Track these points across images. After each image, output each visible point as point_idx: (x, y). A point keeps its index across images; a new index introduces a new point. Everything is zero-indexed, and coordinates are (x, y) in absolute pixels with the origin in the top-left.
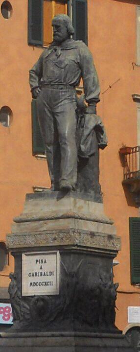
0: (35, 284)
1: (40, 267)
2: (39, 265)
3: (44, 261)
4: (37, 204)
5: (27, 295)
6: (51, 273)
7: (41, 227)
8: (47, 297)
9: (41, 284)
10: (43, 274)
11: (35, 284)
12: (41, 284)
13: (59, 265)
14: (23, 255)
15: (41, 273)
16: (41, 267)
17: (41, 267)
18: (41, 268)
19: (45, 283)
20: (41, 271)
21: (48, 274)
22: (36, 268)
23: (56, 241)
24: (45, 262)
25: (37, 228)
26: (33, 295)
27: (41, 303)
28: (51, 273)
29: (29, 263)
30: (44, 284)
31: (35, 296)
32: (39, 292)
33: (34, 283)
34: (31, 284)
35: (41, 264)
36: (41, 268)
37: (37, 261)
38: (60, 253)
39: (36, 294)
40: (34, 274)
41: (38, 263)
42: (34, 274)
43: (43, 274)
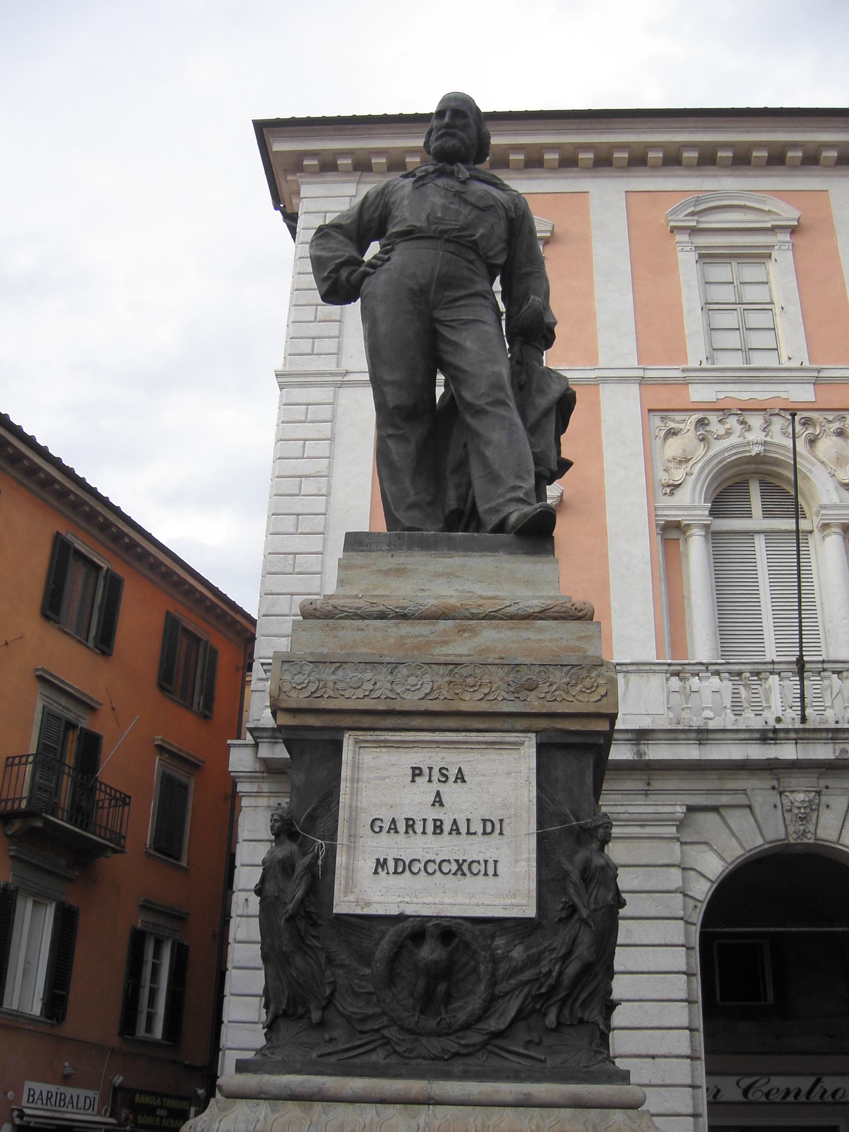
0: (403, 867)
2: (424, 791)
3: (453, 773)
4: (400, 572)
5: (358, 911)
6: (491, 827)
7: (446, 643)
8: (468, 925)
11: (403, 867)
14: (348, 742)
15: (438, 828)
16: (438, 794)
17: (438, 794)
18: (438, 801)
21: (477, 827)
22: (415, 800)
23: (532, 697)
24: (460, 777)
25: (429, 644)
26: (395, 912)
27: (429, 952)
28: (491, 827)
29: (377, 780)
30: (454, 867)
32: (429, 900)
33: (396, 860)
34: (381, 864)
35: (436, 786)
36: (438, 801)
37: (416, 772)
38: (541, 748)
39: (409, 911)
40: (401, 827)
41: (422, 781)
42: (401, 827)
43: (447, 827)
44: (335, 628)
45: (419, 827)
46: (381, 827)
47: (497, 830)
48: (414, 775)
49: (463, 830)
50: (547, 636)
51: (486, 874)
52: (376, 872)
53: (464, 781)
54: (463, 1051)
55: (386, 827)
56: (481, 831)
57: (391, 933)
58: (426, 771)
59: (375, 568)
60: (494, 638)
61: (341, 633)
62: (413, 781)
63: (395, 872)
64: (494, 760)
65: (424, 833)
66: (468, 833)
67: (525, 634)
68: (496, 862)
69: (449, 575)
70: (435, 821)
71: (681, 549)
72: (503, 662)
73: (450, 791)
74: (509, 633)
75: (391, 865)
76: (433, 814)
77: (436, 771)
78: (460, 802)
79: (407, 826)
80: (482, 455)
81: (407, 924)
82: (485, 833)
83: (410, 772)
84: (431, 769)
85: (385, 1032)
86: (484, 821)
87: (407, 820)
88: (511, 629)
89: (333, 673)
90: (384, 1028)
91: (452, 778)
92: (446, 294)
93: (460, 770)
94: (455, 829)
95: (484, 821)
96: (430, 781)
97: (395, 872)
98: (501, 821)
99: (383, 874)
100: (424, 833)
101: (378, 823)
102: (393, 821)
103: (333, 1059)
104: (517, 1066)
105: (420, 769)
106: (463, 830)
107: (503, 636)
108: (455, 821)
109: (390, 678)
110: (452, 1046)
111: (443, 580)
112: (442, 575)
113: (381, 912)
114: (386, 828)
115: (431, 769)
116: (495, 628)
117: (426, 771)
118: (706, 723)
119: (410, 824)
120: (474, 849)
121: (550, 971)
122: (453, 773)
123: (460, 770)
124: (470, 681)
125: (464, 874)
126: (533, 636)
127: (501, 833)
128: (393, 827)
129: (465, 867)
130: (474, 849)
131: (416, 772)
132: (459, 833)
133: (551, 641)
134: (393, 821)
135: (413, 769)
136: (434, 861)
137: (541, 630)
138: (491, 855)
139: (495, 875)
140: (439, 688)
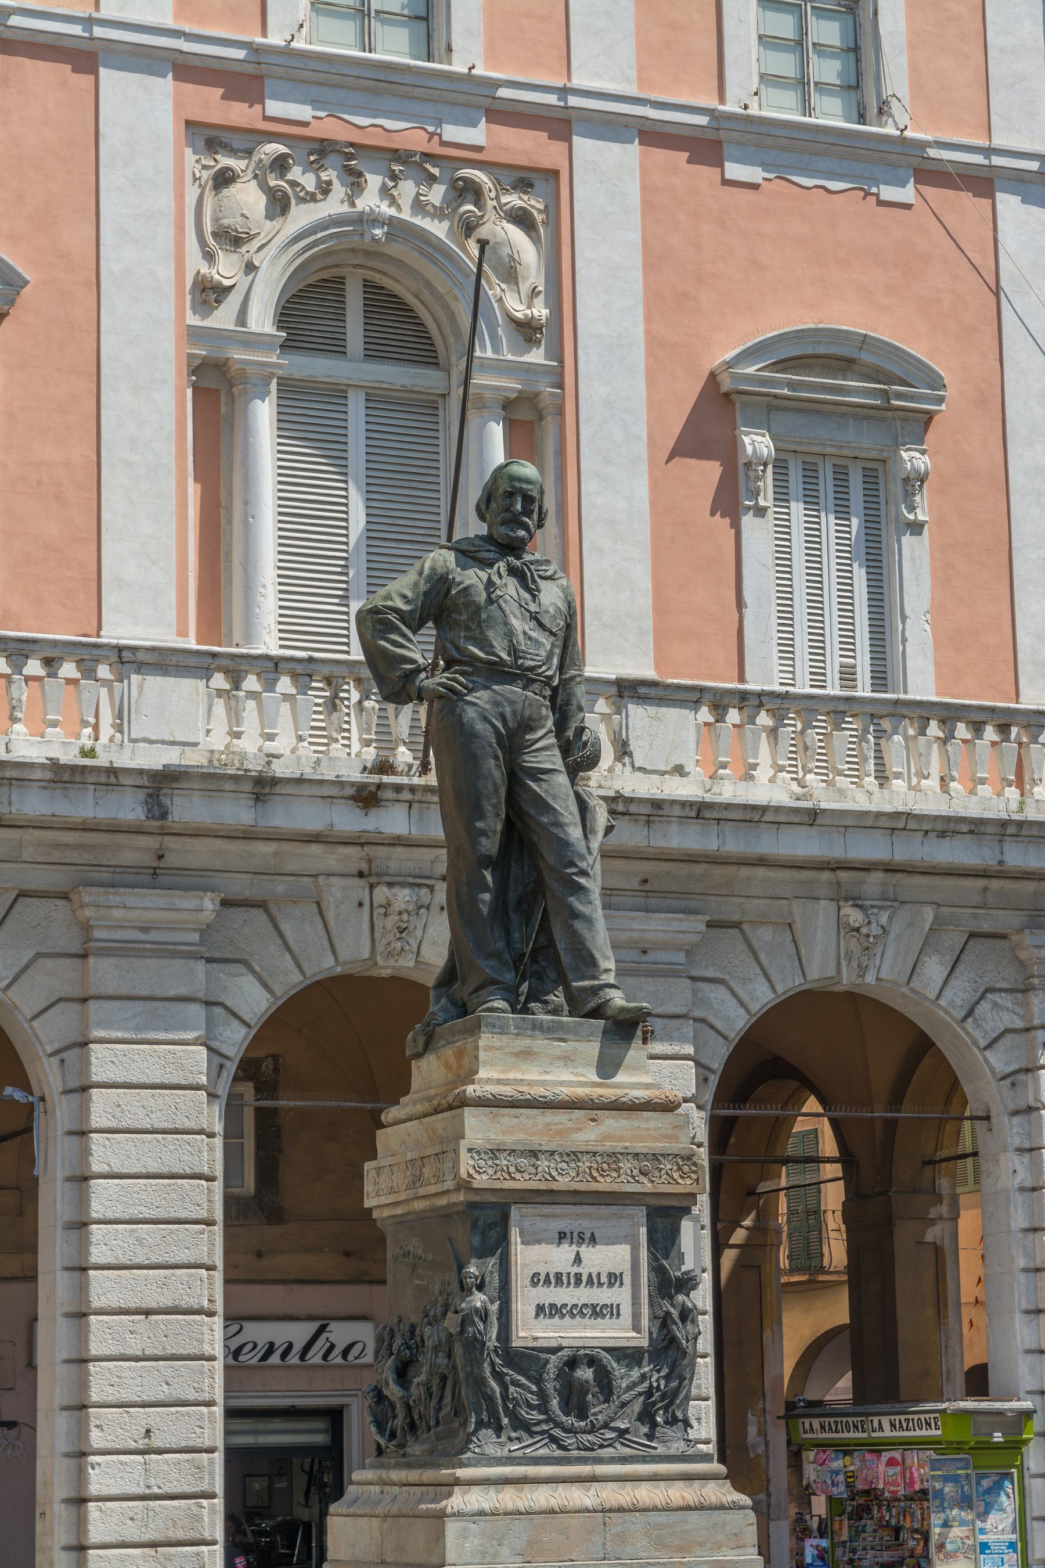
0: (554, 1311)
3: (588, 1235)
4: (526, 1055)
6: (614, 1279)
7: (580, 1129)
9: (577, 1311)
10: (584, 1278)
11: (554, 1311)
12: (577, 1311)
15: (578, 1278)
16: (578, 1253)
17: (578, 1253)
18: (578, 1260)
19: (594, 1307)
20: (576, 1270)
21: (604, 1279)
25: (569, 1131)
26: (554, 1344)
28: (614, 1279)
31: (560, 1348)
33: (552, 1306)
34: (540, 1309)
36: (578, 1260)
43: (584, 1278)
44: (497, 1116)
45: (565, 1279)
46: (539, 1280)
47: (618, 1283)
48: (560, 1238)
50: (651, 1125)
54: (605, 1443)
55: (542, 1278)
58: (569, 1235)
59: (507, 1050)
61: (502, 1120)
63: (551, 1314)
64: (615, 1226)
67: (636, 1124)
68: (618, 1305)
70: (576, 1274)
71: (223, 410)
72: (627, 1151)
73: (585, 1250)
74: (625, 1122)
77: (575, 1235)
83: (557, 1236)
84: (572, 1233)
85: (551, 1432)
87: (557, 1273)
88: (625, 1118)
90: (551, 1429)
91: (587, 1241)
92: (527, 737)
93: (592, 1234)
94: (590, 1282)
98: (621, 1274)
102: (548, 1275)
104: (641, 1453)
105: (565, 1233)
107: (619, 1124)
109: (547, 1163)
111: (561, 1063)
112: (560, 1058)
113: (545, 1345)
115: (572, 1233)
116: (614, 1118)
117: (569, 1235)
118: (269, 763)
119: (559, 1276)
121: (659, 1385)
123: (592, 1234)
124: (605, 1166)
126: (644, 1126)
128: (547, 1281)
130: (603, 1296)
133: (654, 1129)
134: (548, 1275)
135: (560, 1233)
136: (577, 1305)
137: (647, 1120)
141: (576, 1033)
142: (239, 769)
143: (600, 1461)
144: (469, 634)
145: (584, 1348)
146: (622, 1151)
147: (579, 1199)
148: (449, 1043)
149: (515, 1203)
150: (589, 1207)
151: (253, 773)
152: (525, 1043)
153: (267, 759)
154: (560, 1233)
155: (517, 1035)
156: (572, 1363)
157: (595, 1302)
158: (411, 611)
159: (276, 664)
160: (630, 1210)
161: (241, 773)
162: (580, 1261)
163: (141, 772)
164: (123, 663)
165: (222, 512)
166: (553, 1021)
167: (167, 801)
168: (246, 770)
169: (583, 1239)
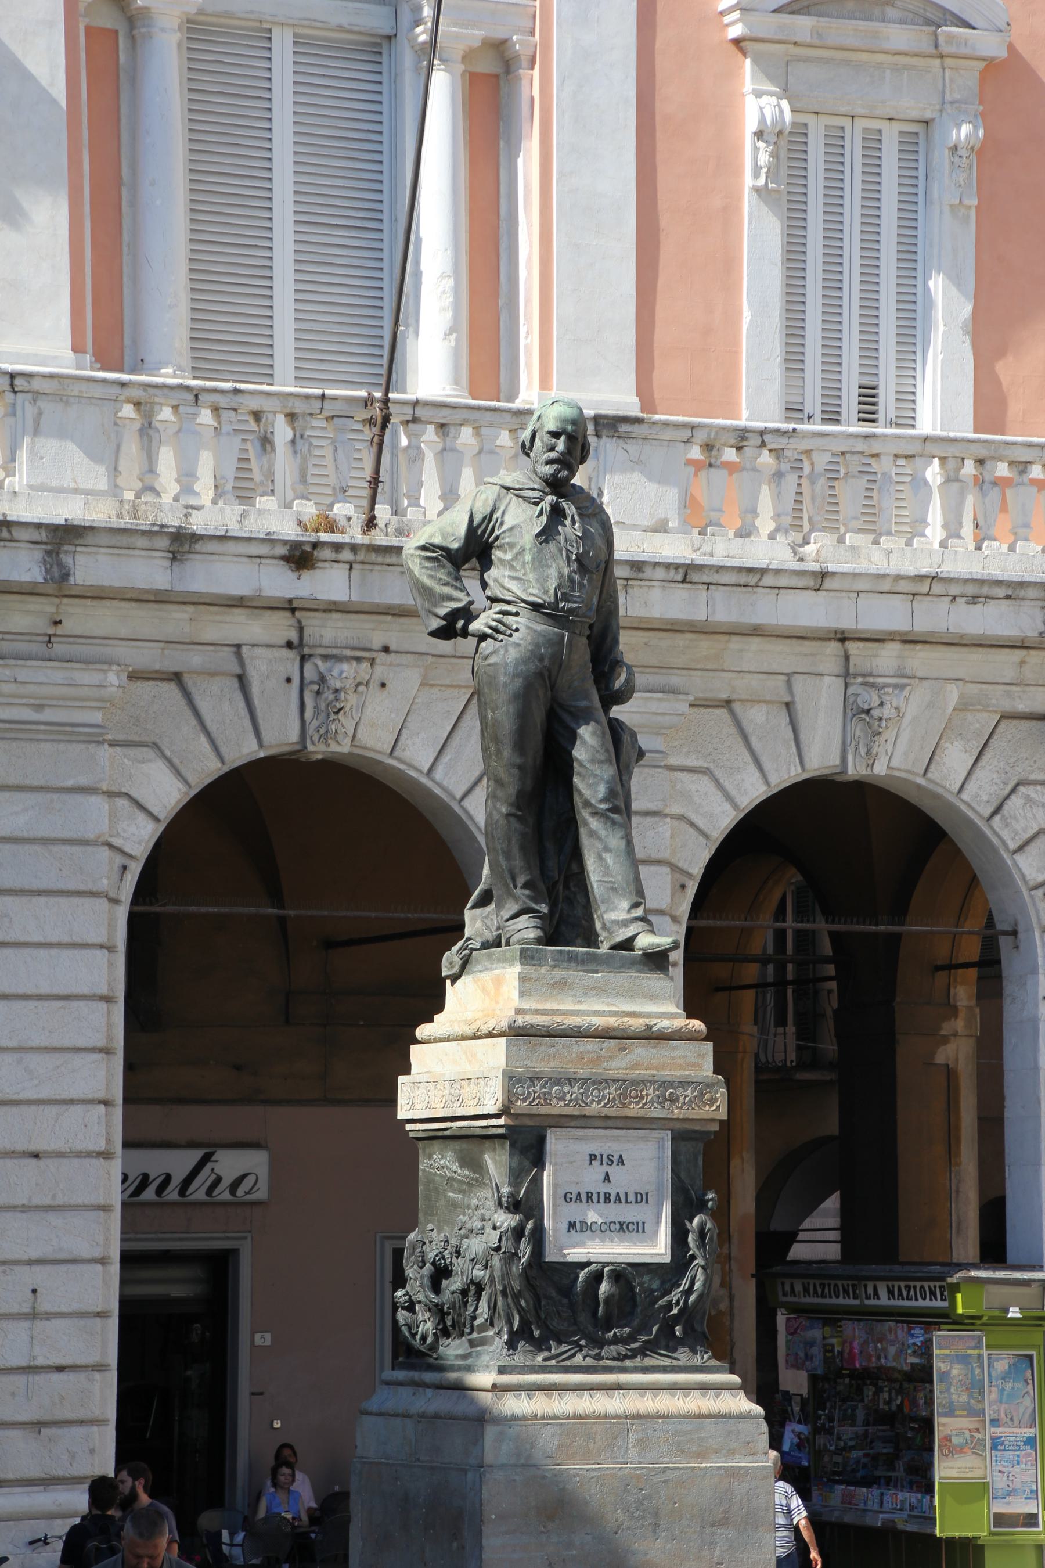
1: (602, 1177)
2: (597, 1171)
3: (615, 1159)
4: (561, 986)
6: (641, 1198)
13: (668, 1174)
16: (607, 1174)
17: (607, 1174)
18: (607, 1178)
22: (591, 1179)
24: (621, 1161)
26: (584, 1260)
28: (641, 1198)
30: (618, 1226)
31: (588, 1264)
35: (605, 1168)
36: (607, 1178)
37: (592, 1157)
38: (673, 1139)
40: (584, 1197)
42: (584, 1197)
43: (613, 1198)
44: (535, 1045)
49: (623, 1200)
51: (638, 1231)
52: (569, 1231)
53: (623, 1164)
55: (574, 1197)
56: (634, 1201)
57: (582, 1274)
58: (599, 1157)
60: (641, 1052)
61: (541, 1049)
62: (591, 1164)
65: (598, 1202)
66: (626, 1202)
67: (663, 1052)
69: (600, 991)
73: (614, 1170)
74: (654, 1051)
75: (578, 1225)
76: (604, 1188)
77: (605, 1157)
78: (623, 1180)
79: (588, 1197)
80: (600, 858)
81: (592, 1267)
82: (636, 1202)
83: (588, 1158)
86: (636, 1194)
87: (587, 1193)
89: (544, 1087)
91: (615, 1162)
93: (621, 1156)
95: (636, 1194)
96: (602, 1164)
97: (582, 1231)
98: (647, 1194)
99: (573, 1232)
100: (598, 1202)
101: (569, 1195)
102: (579, 1194)
103: (553, 1362)
106: (623, 1200)
108: (618, 1194)
110: (621, 1349)
114: (574, 1199)
117: (599, 1157)
119: (589, 1196)
120: (631, 1213)
122: (615, 1159)
125: (624, 1231)
127: (647, 1202)
129: (624, 1226)
130: (631, 1213)
131: (592, 1157)
132: (620, 1202)
134: (579, 1194)
135: (591, 1155)
138: (640, 1218)
139: (644, 1231)
140: (614, 1098)
141: (608, 965)
142: (154, 525)
143: (624, 1370)
144: (514, 574)
145: (612, 1263)
146: (651, 1079)
147: (610, 1123)
148: (487, 969)
149: (550, 1127)
150: (618, 1131)
151: (171, 530)
152: (559, 974)
153: (185, 511)
154: (591, 1155)
155: (555, 966)
156: (597, 1277)
157: (622, 1220)
158: (458, 550)
159: (196, 396)
160: (656, 1134)
161: (156, 528)
162: (609, 1181)
163: (39, 526)
164: (15, 392)
165: (125, 192)
166: (587, 953)
167: (67, 560)
168: (162, 526)
169: (612, 1161)
